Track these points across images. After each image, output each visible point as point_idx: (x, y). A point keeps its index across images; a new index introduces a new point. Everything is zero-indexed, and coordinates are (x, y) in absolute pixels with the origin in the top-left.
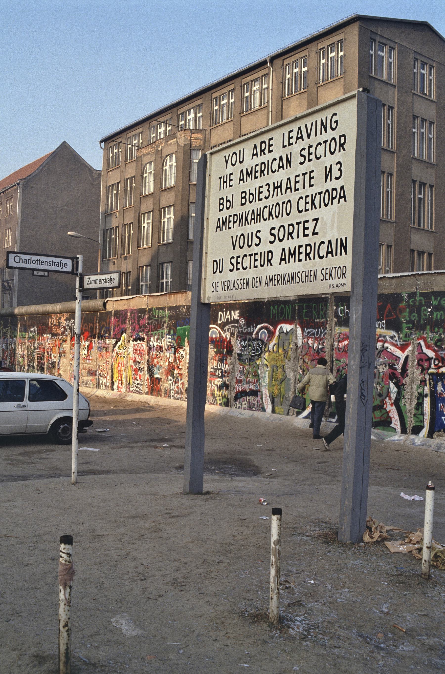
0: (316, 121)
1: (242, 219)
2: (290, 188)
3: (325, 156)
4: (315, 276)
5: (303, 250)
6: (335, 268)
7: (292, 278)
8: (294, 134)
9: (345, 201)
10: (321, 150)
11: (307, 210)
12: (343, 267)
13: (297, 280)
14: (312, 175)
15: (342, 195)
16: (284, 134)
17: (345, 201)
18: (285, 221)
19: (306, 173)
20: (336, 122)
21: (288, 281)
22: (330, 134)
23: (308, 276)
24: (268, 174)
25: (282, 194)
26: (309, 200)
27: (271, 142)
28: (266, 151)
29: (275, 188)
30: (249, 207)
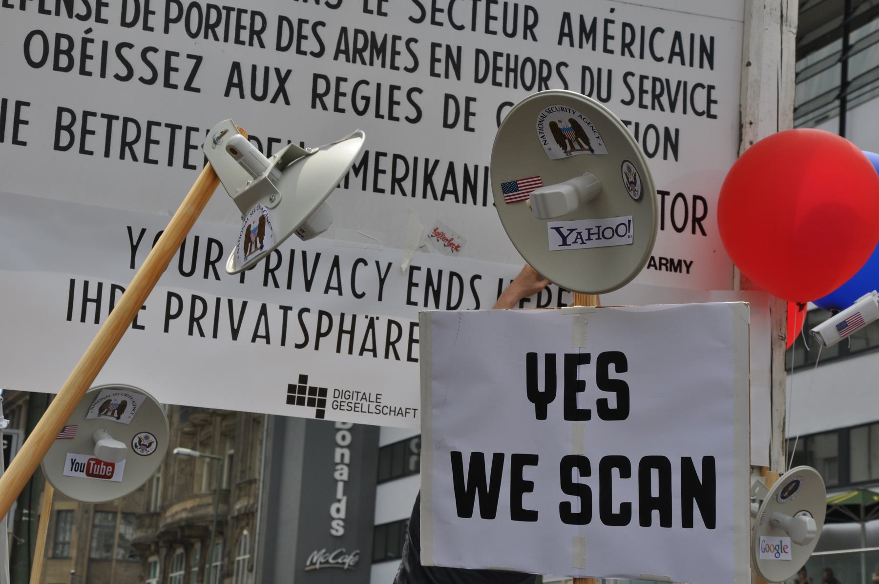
12: (696, 198)
21: (445, 191)
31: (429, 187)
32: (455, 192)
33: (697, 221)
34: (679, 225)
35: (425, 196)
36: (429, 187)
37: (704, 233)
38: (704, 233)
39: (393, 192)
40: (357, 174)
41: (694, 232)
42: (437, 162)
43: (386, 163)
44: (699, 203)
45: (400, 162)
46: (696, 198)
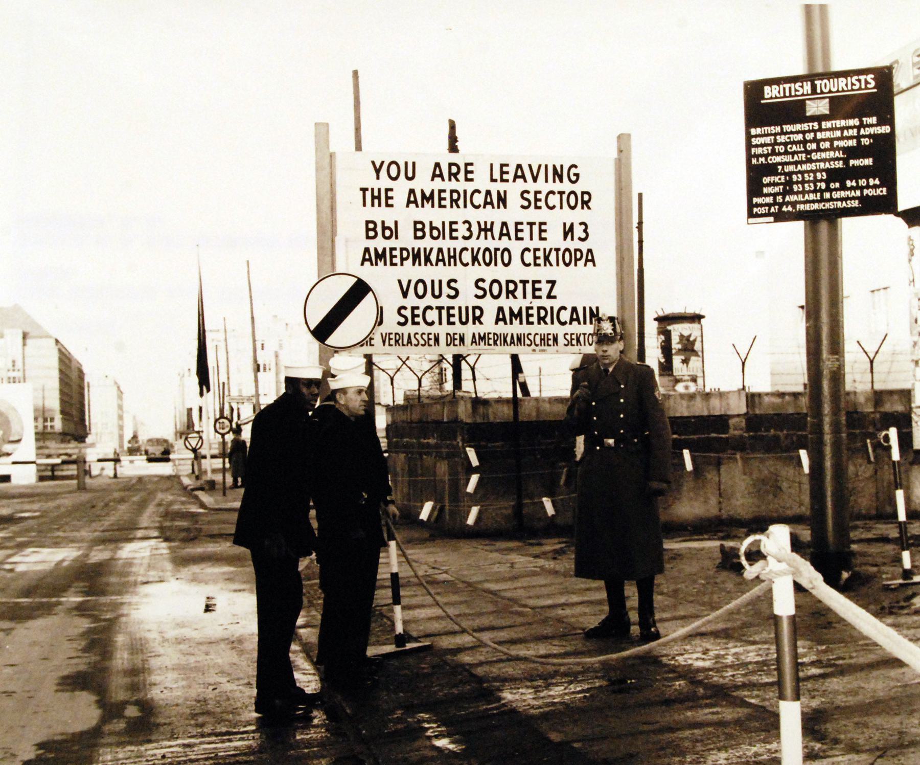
0: (546, 166)
1: (416, 256)
2: (508, 235)
5: (534, 312)
8: (511, 169)
10: (554, 200)
11: (536, 265)
14: (543, 227)
15: (590, 257)
16: (492, 165)
17: (594, 265)
18: (499, 272)
19: (534, 223)
20: (577, 175)
25: (493, 238)
26: (540, 254)
27: (469, 168)
28: (461, 176)
29: (480, 230)
30: (427, 243)
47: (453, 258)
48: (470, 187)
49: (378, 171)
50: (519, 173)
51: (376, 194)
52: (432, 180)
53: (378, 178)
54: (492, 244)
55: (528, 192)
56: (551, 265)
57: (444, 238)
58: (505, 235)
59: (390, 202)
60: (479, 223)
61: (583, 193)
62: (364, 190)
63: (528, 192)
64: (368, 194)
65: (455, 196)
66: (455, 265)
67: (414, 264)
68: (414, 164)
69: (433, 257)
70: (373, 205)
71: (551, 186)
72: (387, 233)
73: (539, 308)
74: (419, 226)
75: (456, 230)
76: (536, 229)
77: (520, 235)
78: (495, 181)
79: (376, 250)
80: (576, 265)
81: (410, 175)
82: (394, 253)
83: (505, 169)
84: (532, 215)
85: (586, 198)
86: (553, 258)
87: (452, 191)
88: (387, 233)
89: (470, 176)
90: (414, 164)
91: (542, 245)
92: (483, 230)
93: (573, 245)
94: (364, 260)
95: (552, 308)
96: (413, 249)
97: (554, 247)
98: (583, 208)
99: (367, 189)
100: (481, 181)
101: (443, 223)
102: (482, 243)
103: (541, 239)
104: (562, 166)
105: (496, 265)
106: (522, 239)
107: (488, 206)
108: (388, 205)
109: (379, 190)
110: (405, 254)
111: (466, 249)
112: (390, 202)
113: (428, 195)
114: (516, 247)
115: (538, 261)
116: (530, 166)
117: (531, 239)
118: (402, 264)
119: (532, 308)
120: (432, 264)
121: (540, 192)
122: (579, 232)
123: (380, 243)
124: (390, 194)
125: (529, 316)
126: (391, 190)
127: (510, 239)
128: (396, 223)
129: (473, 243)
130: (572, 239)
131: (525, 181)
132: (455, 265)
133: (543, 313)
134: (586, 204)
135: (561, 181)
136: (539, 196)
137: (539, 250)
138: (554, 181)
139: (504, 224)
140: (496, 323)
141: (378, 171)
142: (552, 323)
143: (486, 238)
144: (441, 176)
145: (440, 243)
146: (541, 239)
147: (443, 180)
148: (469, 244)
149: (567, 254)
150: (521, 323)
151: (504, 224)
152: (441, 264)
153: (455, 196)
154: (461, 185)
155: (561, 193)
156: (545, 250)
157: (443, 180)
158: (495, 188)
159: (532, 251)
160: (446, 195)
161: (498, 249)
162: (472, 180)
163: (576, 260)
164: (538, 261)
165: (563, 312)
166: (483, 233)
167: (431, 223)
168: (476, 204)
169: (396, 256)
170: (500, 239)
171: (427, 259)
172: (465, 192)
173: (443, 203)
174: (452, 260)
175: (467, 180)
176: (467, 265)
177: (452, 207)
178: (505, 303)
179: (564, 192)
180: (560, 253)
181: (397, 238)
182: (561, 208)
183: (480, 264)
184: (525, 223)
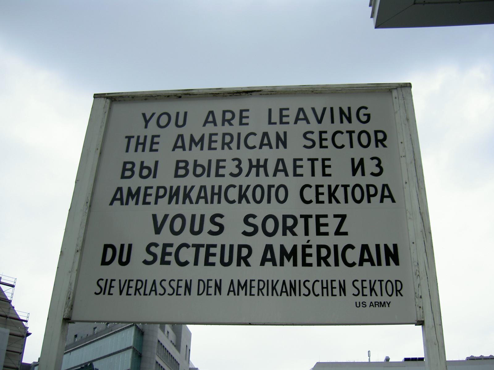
0: (332, 109)
1: (174, 195)
2: (285, 170)
3: (352, 146)
4: (343, 289)
5: (313, 251)
6: (381, 281)
7: (293, 288)
8: (292, 114)
9: (393, 201)
10: (341, 139)
11: (318, 202)
12: (396, 281)
13: (304, 291)
14: (327, 163)
15: (386, 193)
16: (270, 110)
17: (393, 201)
19: (317, 160)
21: (282, 292)
22: (356, 126)
23: (327, 288)
24: (238, 148)
25: (267, 175)
26: (325, 190)
27: (244, 114)
28: (236, 121)
30: (190, 181)
31: (274, 291)
32: (286, 292)
33: (397, 291)
34: (390, 294)
35: (272, 295)
36: (274, 291)
37: (402, 295)
38: (402, 295)
39: (258, 295)
40: (242, 289)
41: (397, 295)
42: (278, 281)
43: (255, 284)
44: (398, 283)
45: (261, 283)
46: (396, 281)
47: (219, 194)
48: (244, 131)
49: (147, 122)
50: (301, 116)
51: (141, 140)
52: (204, 125)
53: (146, 127)
54: (264, 181)
55: (312, 133)
56: (338, 202)
57: (209, 176)
58: (281, 171)
59: (155, 147)
60: (250, 161)
61: (376, 132)
62: (129, 138)
63: (312, 133)
64: (133, 142)
65: (228, 139)
66: (219, 202)
67: (170, 202)
68: (186, 113)
69: (194, 195)
70: (136, 150)
71: (337, 126)
72: (145, 172)
73: (319, 247)
74: (182, 165)
75: (224, 167)
76: (318, 165)
77: (299, 171)
78: (275, 123)
79: (129, 189)
80: (369, 201)
81: (180, 122)
82: (149, 191)
83: (285, 113)
84: (317, 153)
85: (380, 136)
86: (340, 194)
87: (224, 135)
88: (145, 172)
89: (244, 121)
90: (186, 113)
91: (326, 181)
92: (254, 166)
93: (363, 181)
94: (114, 199)
95: (336, 247)
96: (171, 188)
97: (340, 184)
98: (377, 146)
99: (133, 137)
100: (258, 123)
101: (210, 161)
102: (252, 180)
103: (324, 174)
104: (349, 109)
105: (269, 201)
106: (301, 175)
107: (264, 147)
108: (151, 150)
109: (146, 137)
110: (162, 192)
111: (234, 186)
112: (155, 147)
113: (197, 139)
114: (294, 184)
115: (321, 198)
116: (313, 109)
117: (313, 175)
118: (156, 203)
119: (310, 246)
120: (191, 202)
121: (326, 132)
122: (370, 166)
123: (135, 183)
124: (156, 140)
125: (305, 255)
126: (159, 136)
127: (287, 175)
128: (157, 163)
129: (242, 181)
130: (363, 174)
131: (308, 122)
132: (219, 202)
133: (324, 252)
134: (381, 142)
135: (350, 121)
136: (324, 136)
137: (322, 186)
138: (342, 122)
139: (280, 161)
140: (262, 264)
141: (147, 122)
142: (337, 264)
143: (258, 175)
144: (214, 122)
145: (204, 180)
146: (324, 174)
147: (215, 125)
148: (236, 181)
149: (357, 190)
150: (295, 264)
151: (280, 161)
152: (202, 201)
153: (228, 139)
154: (235, 129)
155: (350, 133)
156: (330, 187)
157: (215, 125)
158: (272, 131)
159: (314, 188)
160: (219, 138)
161: (273, 186)
162: (247, 124)
163: (369, 196)
164: (321, 198)
165: (349, 251)
166: (254, 170)
167: (196, 161)
168: (250, 144)
169: (150, 195)
170: (275, 175)
171: (187, 196)
172: (239, 134)
173: (213, 145)
174: (216, 197)
175: (241, 123)
176: (234, 202)
177: (223, 148)
178: (277, 241)
179: (354, 132)
180: (349, 190)
181: (155, 177)
182: (352, 146)
183: (248, 202)
184: (305, 160)
